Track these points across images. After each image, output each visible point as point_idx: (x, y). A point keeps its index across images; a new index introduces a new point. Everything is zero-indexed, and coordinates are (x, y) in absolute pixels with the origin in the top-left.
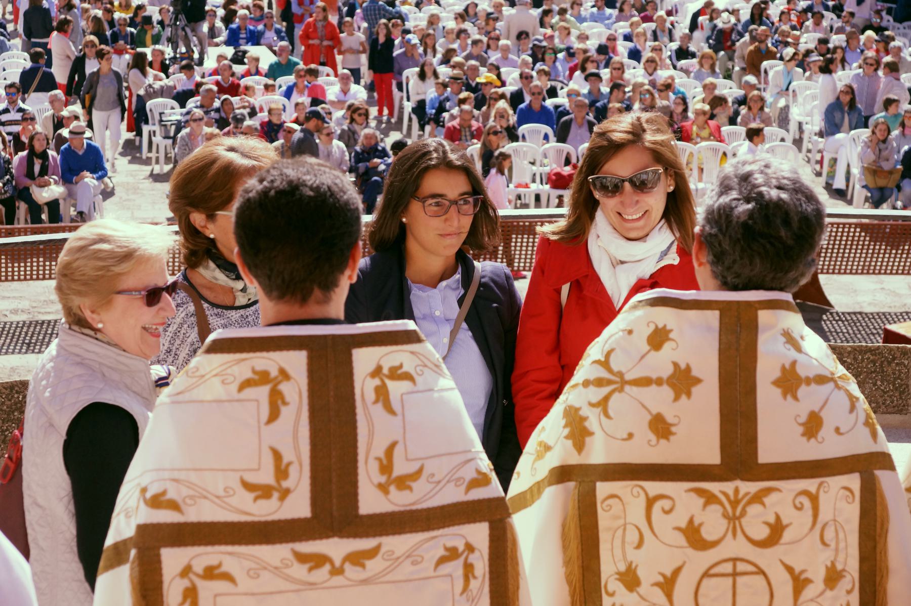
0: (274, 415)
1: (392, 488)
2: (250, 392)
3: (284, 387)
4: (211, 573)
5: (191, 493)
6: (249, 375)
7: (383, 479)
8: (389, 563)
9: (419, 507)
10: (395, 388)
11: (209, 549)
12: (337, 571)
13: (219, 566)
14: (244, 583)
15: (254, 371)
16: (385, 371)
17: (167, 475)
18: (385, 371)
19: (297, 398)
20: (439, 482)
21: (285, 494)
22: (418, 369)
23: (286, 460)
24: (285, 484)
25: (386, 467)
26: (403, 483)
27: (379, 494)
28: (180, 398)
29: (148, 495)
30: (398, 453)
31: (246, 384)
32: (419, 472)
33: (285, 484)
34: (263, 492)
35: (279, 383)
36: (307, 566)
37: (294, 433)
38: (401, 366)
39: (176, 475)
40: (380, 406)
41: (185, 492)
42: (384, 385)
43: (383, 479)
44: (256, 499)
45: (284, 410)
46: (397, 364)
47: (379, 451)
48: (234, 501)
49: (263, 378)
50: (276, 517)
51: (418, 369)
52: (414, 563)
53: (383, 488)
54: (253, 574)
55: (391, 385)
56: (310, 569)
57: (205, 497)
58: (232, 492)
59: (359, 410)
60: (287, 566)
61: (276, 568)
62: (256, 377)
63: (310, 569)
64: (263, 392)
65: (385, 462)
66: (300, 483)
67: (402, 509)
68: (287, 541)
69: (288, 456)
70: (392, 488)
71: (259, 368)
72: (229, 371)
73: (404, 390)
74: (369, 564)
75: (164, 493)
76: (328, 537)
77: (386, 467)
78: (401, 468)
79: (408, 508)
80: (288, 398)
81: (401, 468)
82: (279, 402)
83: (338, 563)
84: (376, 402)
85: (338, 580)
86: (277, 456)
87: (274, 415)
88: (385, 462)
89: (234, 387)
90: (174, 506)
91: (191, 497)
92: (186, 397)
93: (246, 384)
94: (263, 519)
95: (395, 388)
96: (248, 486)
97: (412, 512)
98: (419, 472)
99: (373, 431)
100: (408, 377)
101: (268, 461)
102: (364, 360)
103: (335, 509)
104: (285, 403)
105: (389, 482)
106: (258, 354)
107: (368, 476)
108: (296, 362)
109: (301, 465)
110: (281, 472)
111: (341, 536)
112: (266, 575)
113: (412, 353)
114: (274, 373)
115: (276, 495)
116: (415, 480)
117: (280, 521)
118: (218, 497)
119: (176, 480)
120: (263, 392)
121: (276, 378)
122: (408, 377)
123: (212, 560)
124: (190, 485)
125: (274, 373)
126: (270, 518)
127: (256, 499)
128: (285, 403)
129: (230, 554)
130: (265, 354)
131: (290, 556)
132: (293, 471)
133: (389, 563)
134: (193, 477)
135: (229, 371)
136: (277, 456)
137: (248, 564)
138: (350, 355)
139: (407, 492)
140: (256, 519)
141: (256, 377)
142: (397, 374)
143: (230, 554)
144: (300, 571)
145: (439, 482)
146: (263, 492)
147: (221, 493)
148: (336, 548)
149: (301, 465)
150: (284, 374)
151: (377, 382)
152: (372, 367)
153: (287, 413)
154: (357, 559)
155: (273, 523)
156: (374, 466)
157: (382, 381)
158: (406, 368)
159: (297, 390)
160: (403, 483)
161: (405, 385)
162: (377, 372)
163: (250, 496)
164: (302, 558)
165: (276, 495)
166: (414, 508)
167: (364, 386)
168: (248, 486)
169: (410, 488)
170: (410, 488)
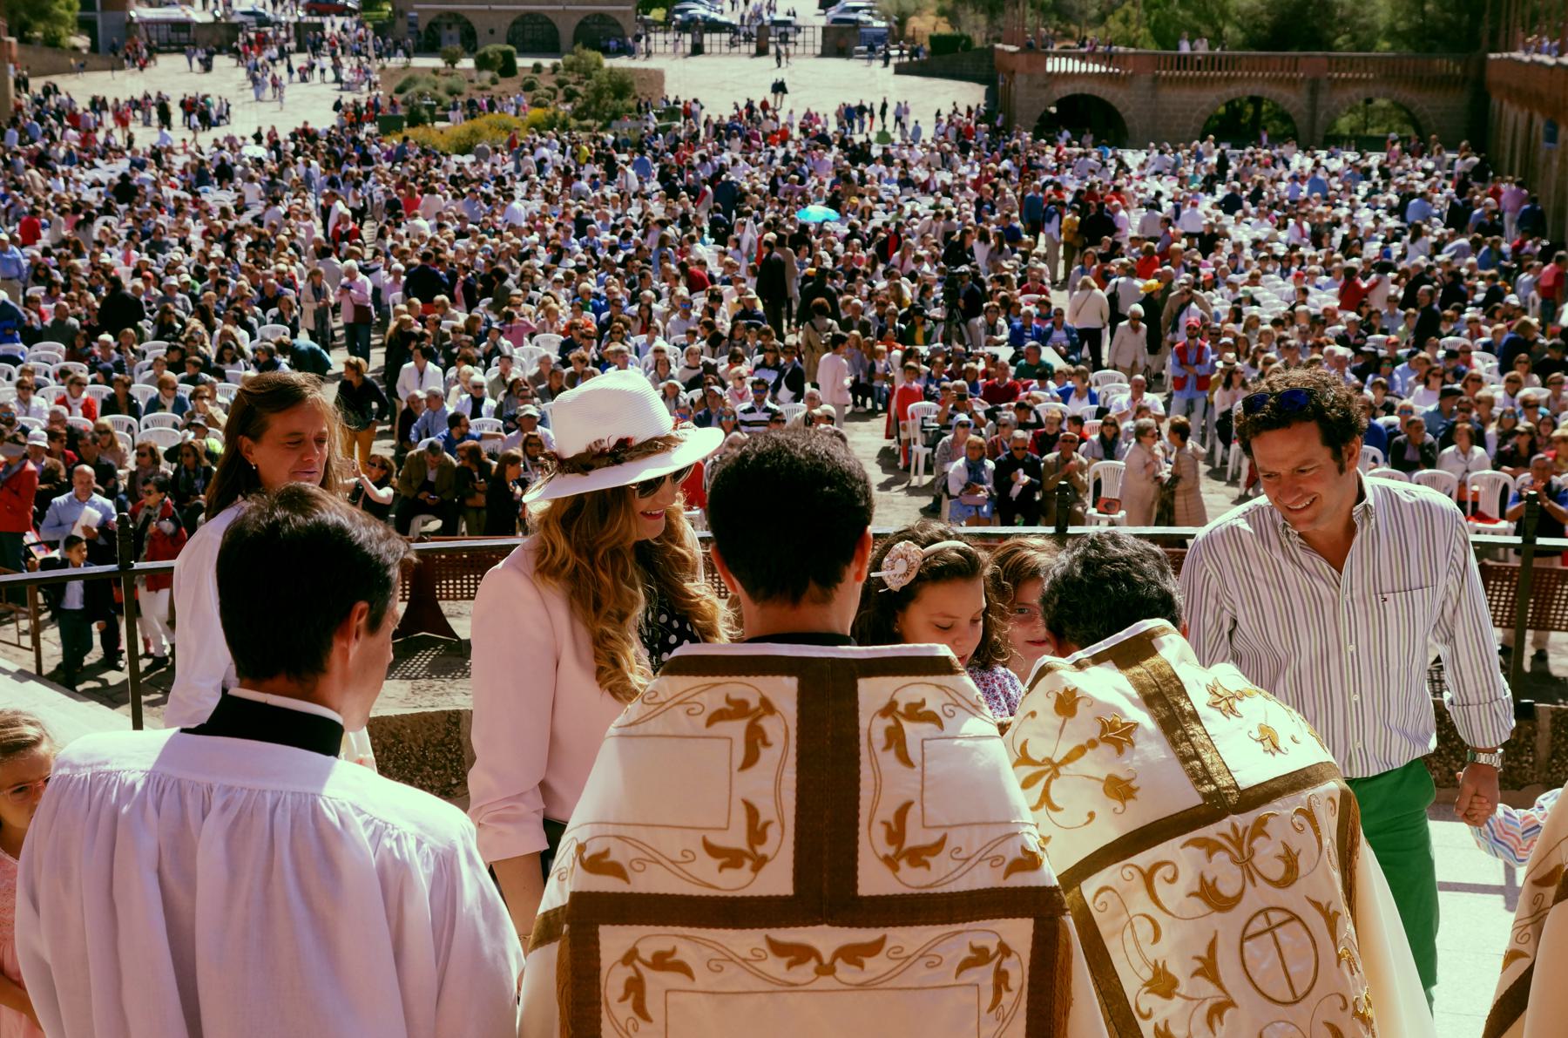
0: (750, 760)
1: (903, 863)
2: (723, 727)
3: (767, 724)
4: (662, 962)
5: (641, 855)
6: (722, 704)
7: (891, 850)
8: (894, 964)
9: (939, 890)
10: (911, 729)
11: (660, 929)
12: (825, 970)
13: (674, 952)
14: (703, 979)
15: (728, 700)
16: (901, 708)
17: (611, 830)
18: (901, 708)
19: (782, 735)
20: (968, 859)
21: (760, 862)
22: (947, 709)
23: (763, 819)
24: (761, 850)
25: (896, 833)
26: (918, 857)
27: (885, 871)
28: (633, 730)
29: (586, 855)
30: (913, 816)
31: (718, 717)
32: (939, 846)
33: (761, 850)
34: (731, 859)
35: (761, 716)
36: (786, 960)
37: (774, 784)
38: (923, 703)
39: (623, 831)
40: (891, 754)
41: (633, 853)
42: (899, 726)
43: (891, 850)
44: (721, 868)
45: (764, 752)
46: (918, 700)
47: (887, 812)
48: (691, 868)
49: (738, 709)
50: (747, 893)
51: (947, 709)
52: (930, 965)
53: (891, 862)
54: (715, 967)
55: (909, 727)
56: (790, 965)
57: (658, 862)
58: (691, 857)
59: (864, 756)
60: (760, 959)
61: (745, 960)
62: (731, 708)
63: (790, 965)
64: (737, 729)
65: (894, 828)
66: (781, 849)
67: (916, 891)
68: (761, 927)
69: (766, 812)
70: (903, 863)
71: (735, 696)
72: (696, 698)
73: (926, 735)
74: (869, 962)
75: (606, 853)
76: (815, 924)
77: (896, 833)
78: (915, 837)
79: (924, 891)
80: (770, 738)
81: (915, 837)
82: (759, 742)
83: (827, 959)
84: (887, 748)
85: (826, 982)
86: (752, 811)
87: (750, 760)
88: (894, 828)
89: (702, 720)
90: (617, 871)
91: (639, 860)
92: (641, 729)
93: (718, 717)
94: (730, 894)
95: (911, 729)
96: (712, 850)
97: (928, 896)
98: (940, 844)
99: (881, 785)
100: (932, 718)
101: (740, 817)
102: (872, 692)
103: (826, 887)
104: (766, 744)
105: (899, 855)
106: (735, 678)
107: (871, 845)
108: (784, 691)
109: (783, 826)
110: (757, 833)
111: (832, 924)
112: (731, 970)
113: (939, 687)
114: (754, 703)
115: (748, 863)
116: (934, 855)
117: (752, 898)
118: (673, 862)
119: (619, 837)
120: (737, 729)
121: (757, 710)
122: (932, 718)
123: (664, 945)
124: (638, 844)
125: (754, 703)
126: (738, 894)
127: (721, 868)
128: (766, 744)
129: (686, 937)
130: (743, 679)
131: (764, 946)
132: (773, 833)
133: (894, 964)
134: (643, 835)
135: (696, 698)
136: (752, 811)
137: (708, 952)
138: (856, 686)
139: (922, 870)
140: (721, 894)
141: (731, 708)
142: (917, 713)
143: (686, 937)
144: (775, 966)
145: (968, 859)
146: (731, 859)
147: (679, 858)
148: (826, 938)
149: (783, 826)
150: (767, 707)
151: (889, 722)
152: (883, 702)
153: (768, 757)
154: (853, 955)
155: (743, 899)
156: (880, 833)
157: (897, 721)
158: (929, 706)
159: (782, 728)
160: (918, 857)
161: (927, 728)
162: (890, 709)
163: (715, 863)
164: (778, 949)
165: (748, 863)
166: (931, 891)
167: (871, 726)
168: (712, 850)
169: (927, 865)
170: (927, 865)
